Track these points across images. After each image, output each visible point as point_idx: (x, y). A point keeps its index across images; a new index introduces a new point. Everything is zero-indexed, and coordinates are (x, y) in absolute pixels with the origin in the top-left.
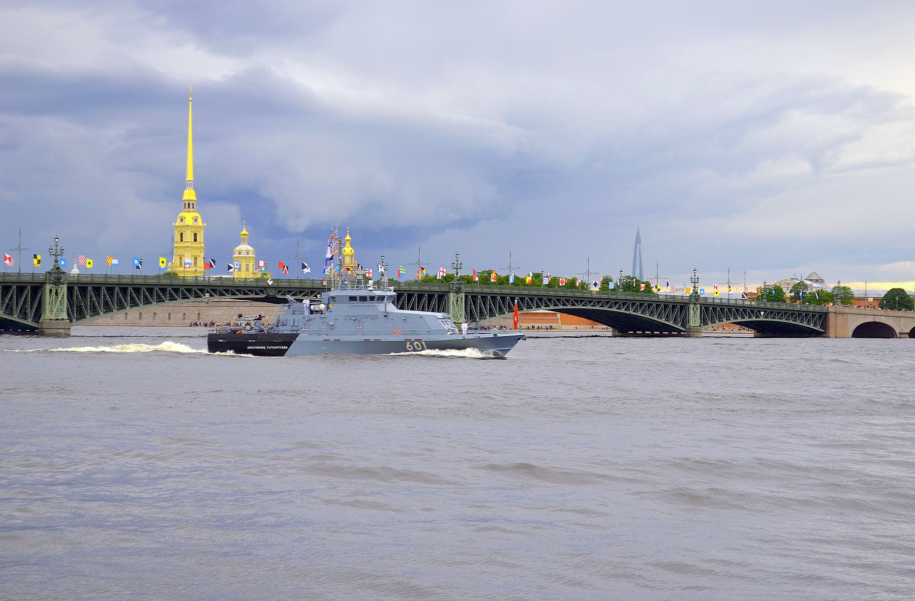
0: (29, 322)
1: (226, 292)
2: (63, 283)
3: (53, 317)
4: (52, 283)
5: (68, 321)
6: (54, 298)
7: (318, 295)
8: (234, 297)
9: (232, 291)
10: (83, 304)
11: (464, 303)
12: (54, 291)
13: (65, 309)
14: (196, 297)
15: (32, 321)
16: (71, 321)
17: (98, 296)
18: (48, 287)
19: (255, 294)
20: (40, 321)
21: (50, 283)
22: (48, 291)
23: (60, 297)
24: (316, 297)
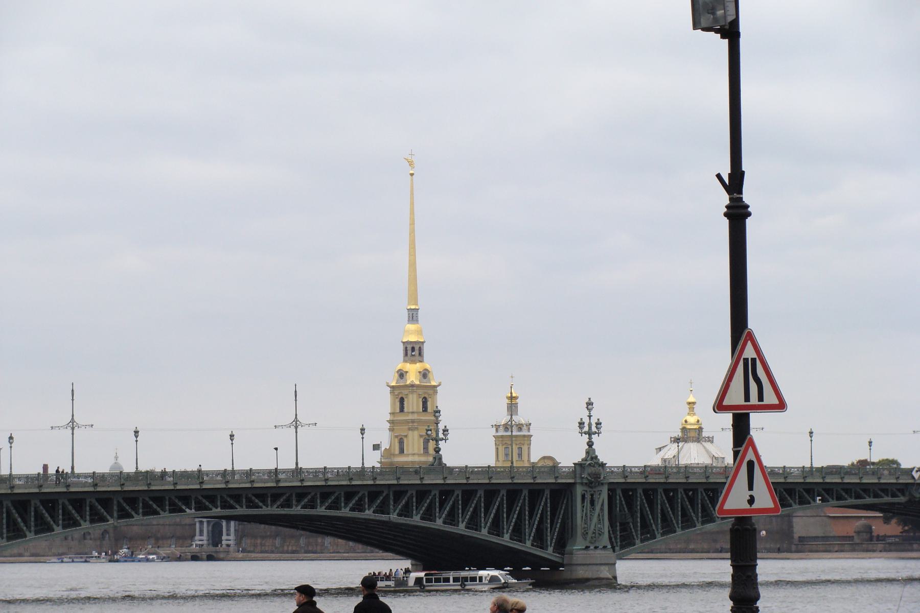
0: (549, 553)
2: (602, 484)
4: (586, 483)
6: (588, 508)
8: (842, 503)
10: (630, 520)
12: (588, 497)
14: (801, 503)
15: (553, 552)
17: (651, 503)
18: (579, 490)
21: (582, 484)
23: (598, 508)
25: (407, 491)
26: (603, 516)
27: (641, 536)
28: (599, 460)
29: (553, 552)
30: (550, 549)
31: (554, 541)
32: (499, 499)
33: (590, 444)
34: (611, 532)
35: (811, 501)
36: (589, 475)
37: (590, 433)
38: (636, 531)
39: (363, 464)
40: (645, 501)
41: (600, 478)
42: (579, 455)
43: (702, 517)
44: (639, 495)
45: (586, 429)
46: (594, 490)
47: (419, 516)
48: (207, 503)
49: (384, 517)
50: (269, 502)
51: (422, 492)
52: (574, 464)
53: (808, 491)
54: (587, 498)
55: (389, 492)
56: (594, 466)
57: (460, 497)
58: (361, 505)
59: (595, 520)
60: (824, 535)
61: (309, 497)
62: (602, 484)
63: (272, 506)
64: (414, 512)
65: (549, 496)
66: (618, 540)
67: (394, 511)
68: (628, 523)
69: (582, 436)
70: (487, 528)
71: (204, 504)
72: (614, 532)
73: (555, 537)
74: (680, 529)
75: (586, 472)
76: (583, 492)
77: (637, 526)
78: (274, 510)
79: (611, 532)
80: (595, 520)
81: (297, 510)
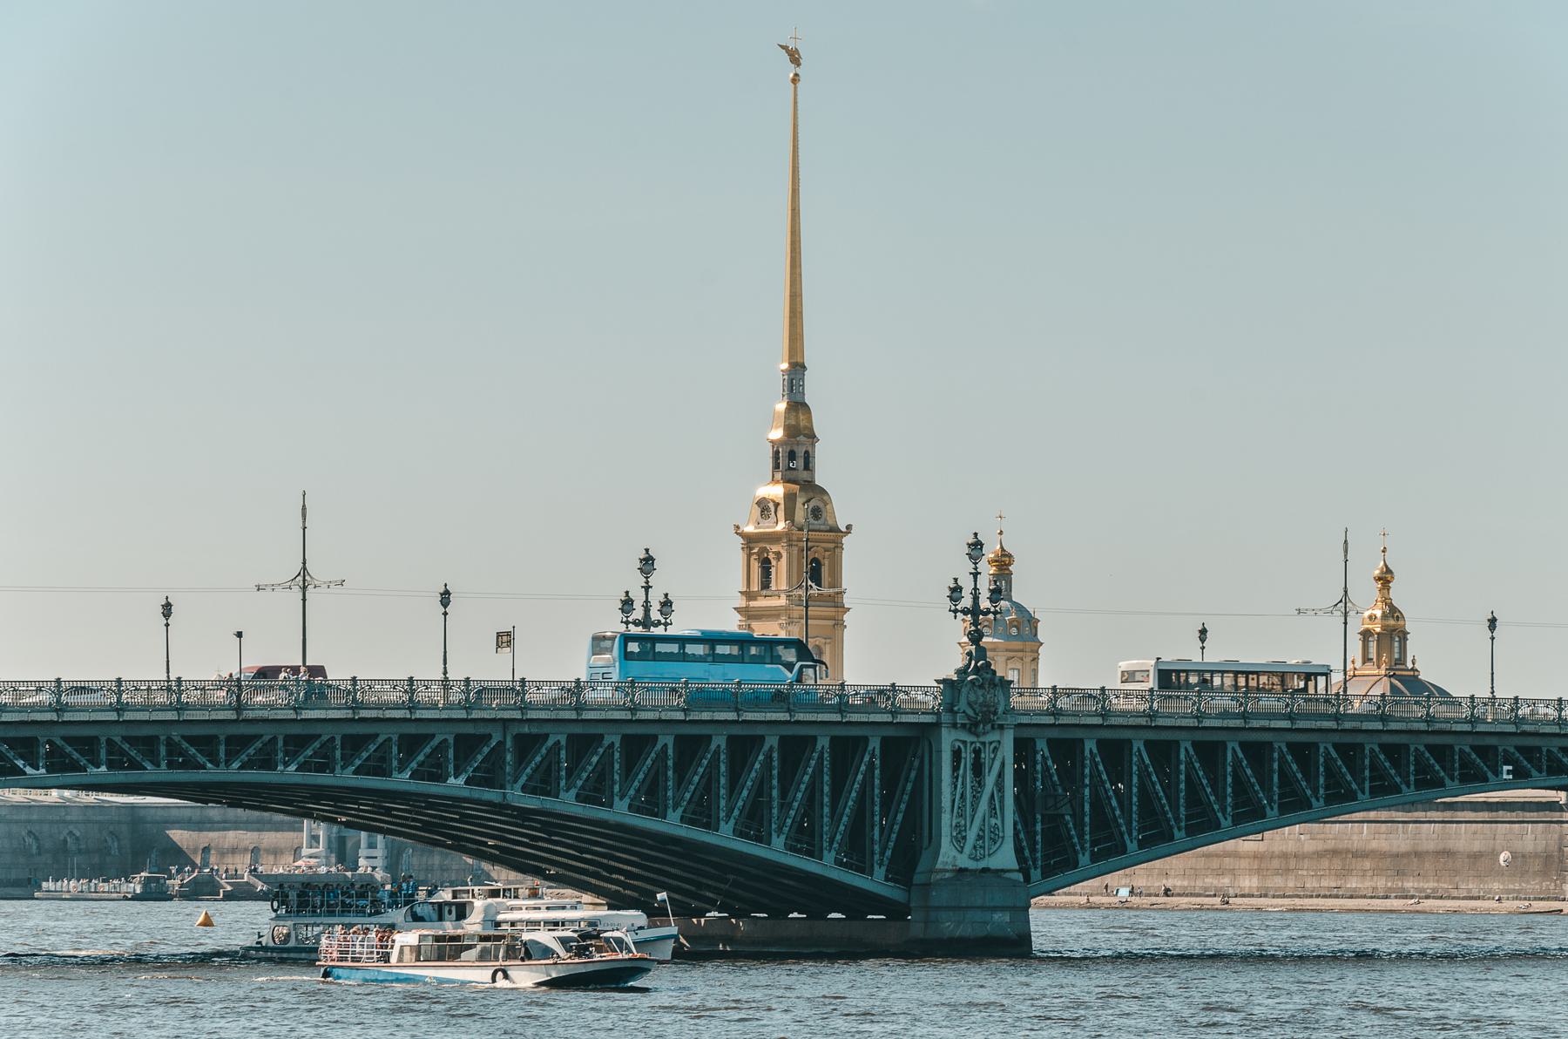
0: (875, 882)
2: (1001, 727)
3: (964, 861)
4: (963, 726)
5: (1020, 877)
15: (887, 879)
18: (948, 739)
20: (917, 879)
21: (954, 725)
22: (946, 758)
23: (990, 781)
25: (546, 736)
28: (994, 672)
30: (879, 873)
31: (889, 853)
32: (761, 757)
34: (1022, 836)
35: (1490, 774)
36: (969, 704)
38: (1081, 836)
40: (1101, 767)
41: (995, 713)
43: (1235, 806)
44: (1087, 753)
46: (982, 739)
47: (573, 792)
48: (76, 755)
49: (492, 795)
50: (222, 755)
52: (936, 681)
53: (1482, 751)
54: (965, 758)
55: (505, 738)
56: (981, 687)
57: (670, 752)
58: (439, 766)
59: (983, 806)
60: (1440, 847)
62: (1001, 727)
63: (228, 763)
64: (563, 783)
65: (877, 752)
66: (1039, 855)
67: (515, 781)
68: (1063, 816)
69: (955, 617)
70: (732, 821)
71: (69, 755)
72: (1031, 835)
73: (891, 844)
75: (963, 701)
76: (957, 744)
77: (1083, 824)
78: (233, 773)
79: (1022, 836)
80: (983, 806)
81: (289, 773)
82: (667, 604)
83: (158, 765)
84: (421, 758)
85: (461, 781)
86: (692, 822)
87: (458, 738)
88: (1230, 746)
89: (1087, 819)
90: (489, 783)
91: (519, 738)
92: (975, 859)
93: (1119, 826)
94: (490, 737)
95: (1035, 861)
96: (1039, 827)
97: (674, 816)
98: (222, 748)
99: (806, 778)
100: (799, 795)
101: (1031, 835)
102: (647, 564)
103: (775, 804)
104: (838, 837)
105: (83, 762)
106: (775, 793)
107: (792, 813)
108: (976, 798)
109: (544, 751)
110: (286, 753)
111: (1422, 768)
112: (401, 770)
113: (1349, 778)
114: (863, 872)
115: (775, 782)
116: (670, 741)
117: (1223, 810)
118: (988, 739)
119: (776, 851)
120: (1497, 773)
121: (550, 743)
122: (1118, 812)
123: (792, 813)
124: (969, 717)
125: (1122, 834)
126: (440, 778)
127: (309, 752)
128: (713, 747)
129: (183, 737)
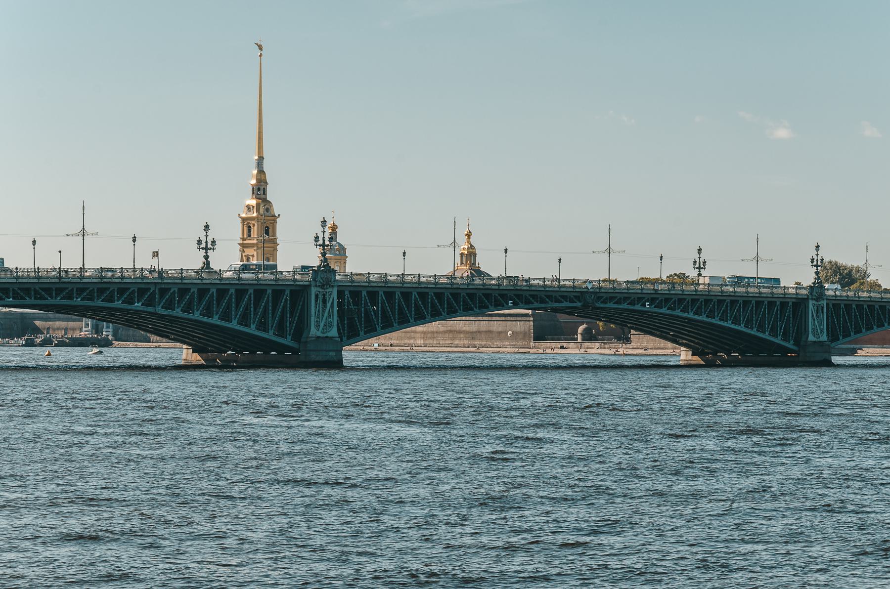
0: (288, 341)
1: (533, 298)
2: (333, 286)
3: (319, 334)
4: (319, 286)
5: (339, 339)
7: (647, 303)
9: (541, 298)
11: (825, 314)
13: (335, 323)
15: (292, 340)
16: (342, 340)
18: (314, 290)
19: (570, 302)
20: (303, 340)
21: (316, 286)
23: (329, 305)
24: (644, 305)
25: (170, 289)
26: (333, 312)
27: (365, 329)
29: (292, 340)
30: (289, 338)
31: (292, 331)
32: (247, 297)
33: (206, 257)
35: (505, 304)
36: (321, 278)
37: (206, 249)
38: (361, 324)
39: (83, 265)
41: (330, 281)
42: (198, 264)
43: (415, 315)
44: (363, 296)
45: (203, 245)
47: (180, 308)
49: (151, 309)
50: (54, 294)
51: (203, 291)
53: (502, 296)
56: (326, 272)
57: (215, 294)
58: (132, 299)
59: (326, 314)
60: (487, 330)
61: (88, 291)
62: (333, 286)
64: (176, 305)
65: (288, 295)
67: (159, 305)
68: (354, 318)
70: (237, 319)
72: (343, 325)
73: (293, 328)
74: (397, 324)
75: (319, 277)
77: (362, 321)
78: (58, 301)
80: (326, 314)
81: (78, 301)
82: (214, 242)
83: (31, 298)
84: (125, 296)
85: (140, 304)
86: (222, 319)
87: (139, 289)
88: (413, 294)
89: (363, 319)
90: (150, 305)
91: (160, 289)
92: (323, 333)
93: (374, 322)
94: (150, 289)
95: (344, 334)
96: (346, 322)
97: (216, 317)
98: (54, 292)
99: (263, 304)
100: (261, 310)
101: (343, 325)
102: (207, 227)
103: (252, 313)
104: (274, 325)
105: (4, 297)
106: (252, 309)
107: (258, 316)
108: (324, 311)
109: (169, 294)
110: (77, 294)
111: (481, 301)
112: (118, 301)
113: (455, 305)
114: (283, 337)
115: (252, 305)
116: (215, 291)
117: (411, 317)
118: (328, 290)
119: (252, 330)
120: (507, 304)
121: (171, 291)
122: (374, 317)
123: (258, 316)
124: (321, 283)
125: (375, 324)
126: (133, 303)
127: (85, 294)
128: (230, 293)
129: (40, 288)
